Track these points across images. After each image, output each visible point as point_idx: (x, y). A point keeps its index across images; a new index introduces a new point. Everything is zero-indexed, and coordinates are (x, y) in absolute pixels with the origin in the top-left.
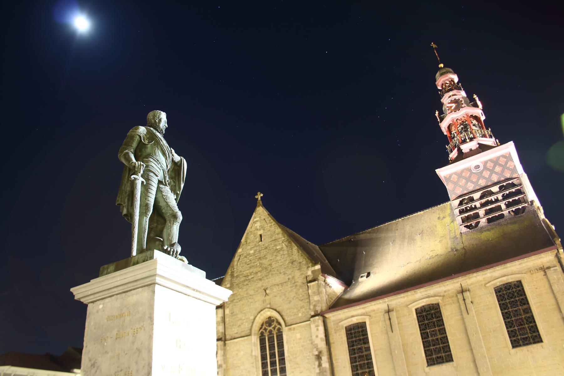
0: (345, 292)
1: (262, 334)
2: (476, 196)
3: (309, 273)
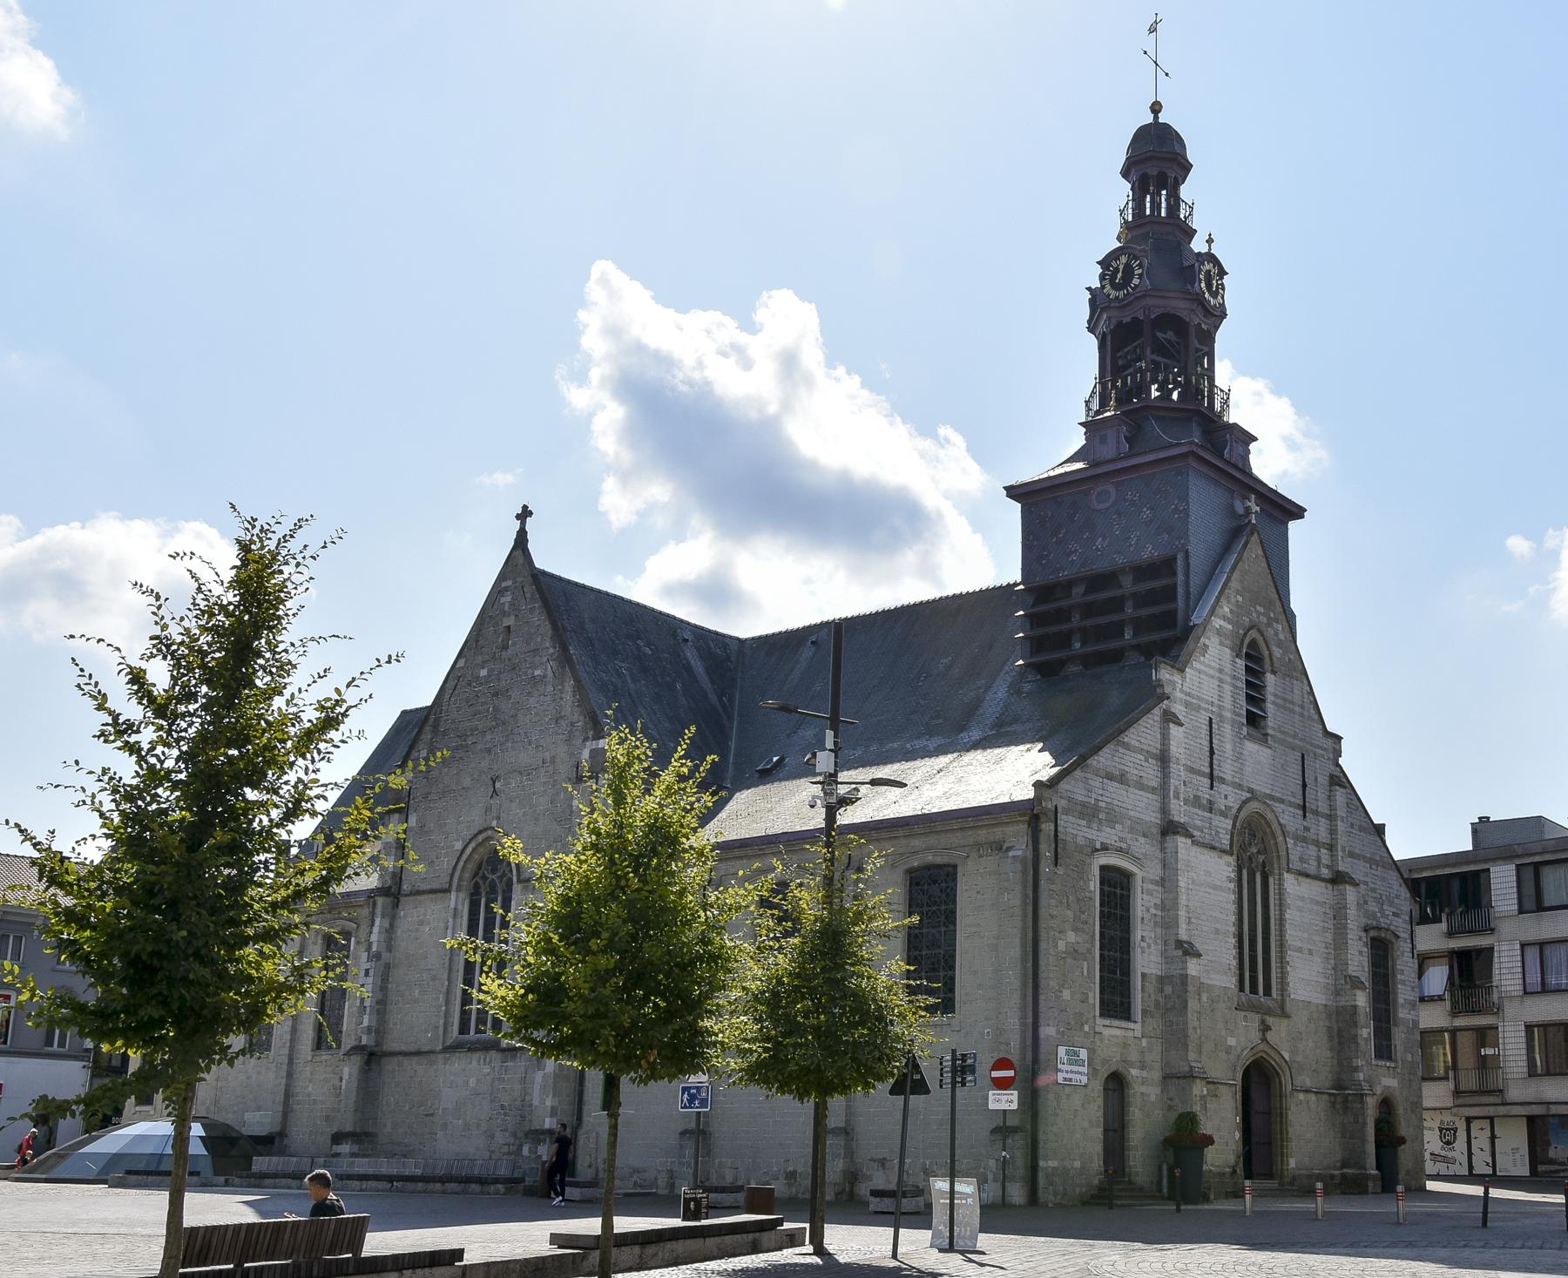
1: (477, 886)
3: (586, 754)
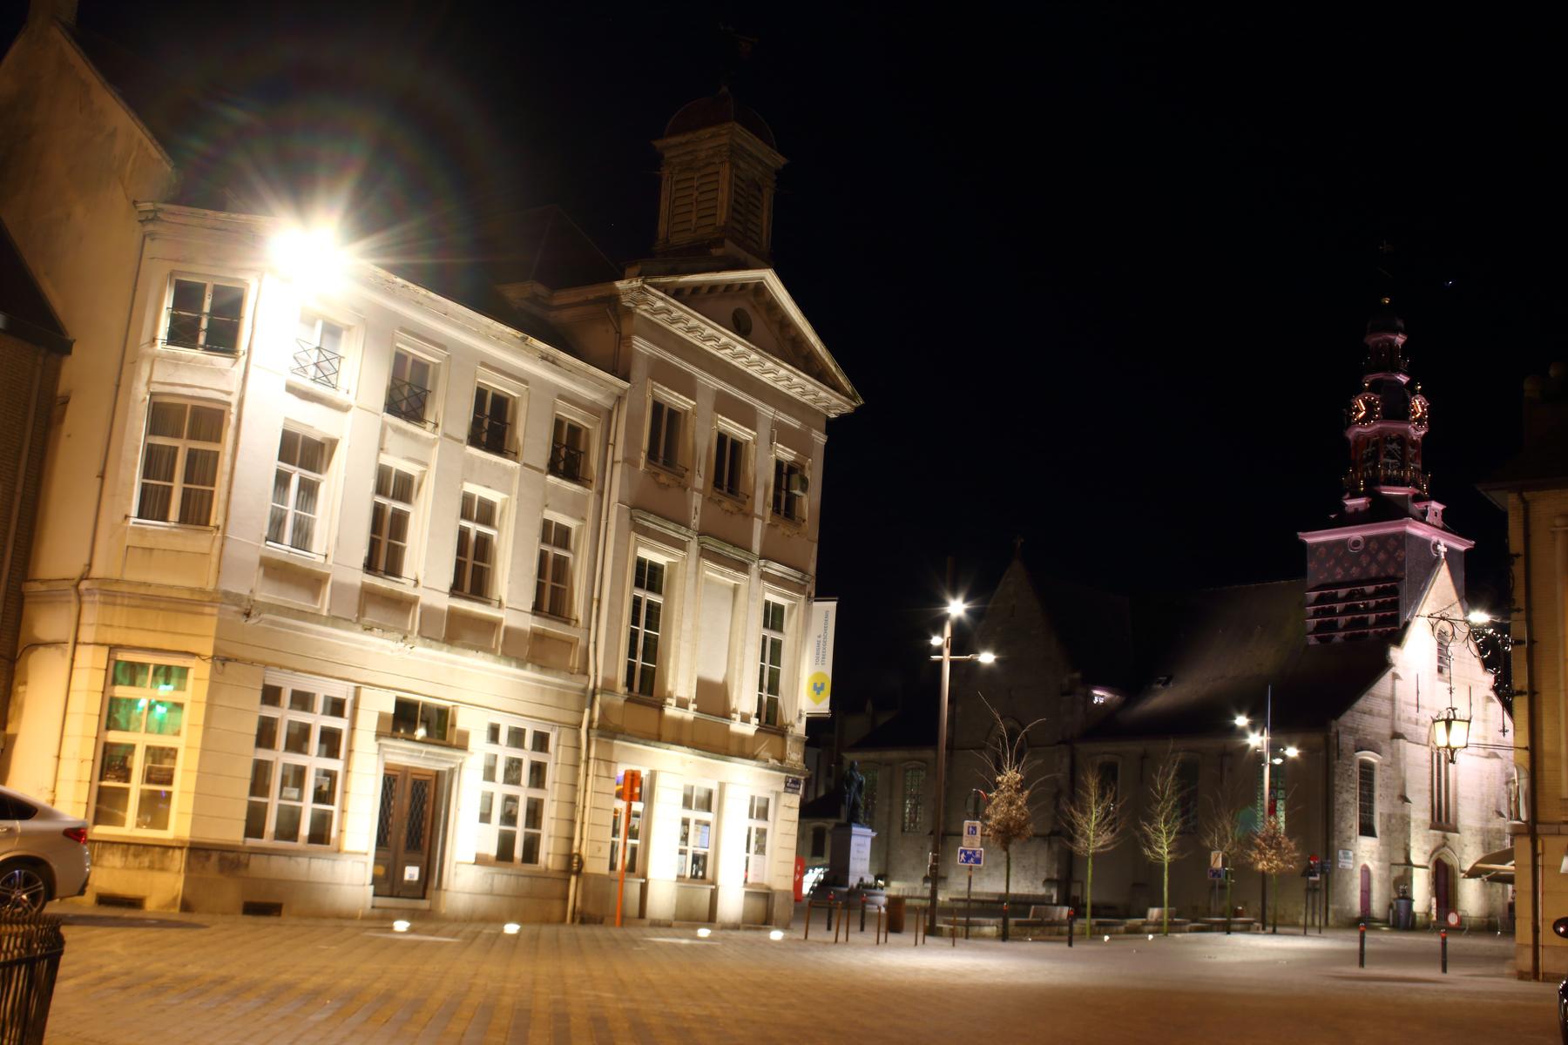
0: (1126, 704)
2: (1342, 592)
